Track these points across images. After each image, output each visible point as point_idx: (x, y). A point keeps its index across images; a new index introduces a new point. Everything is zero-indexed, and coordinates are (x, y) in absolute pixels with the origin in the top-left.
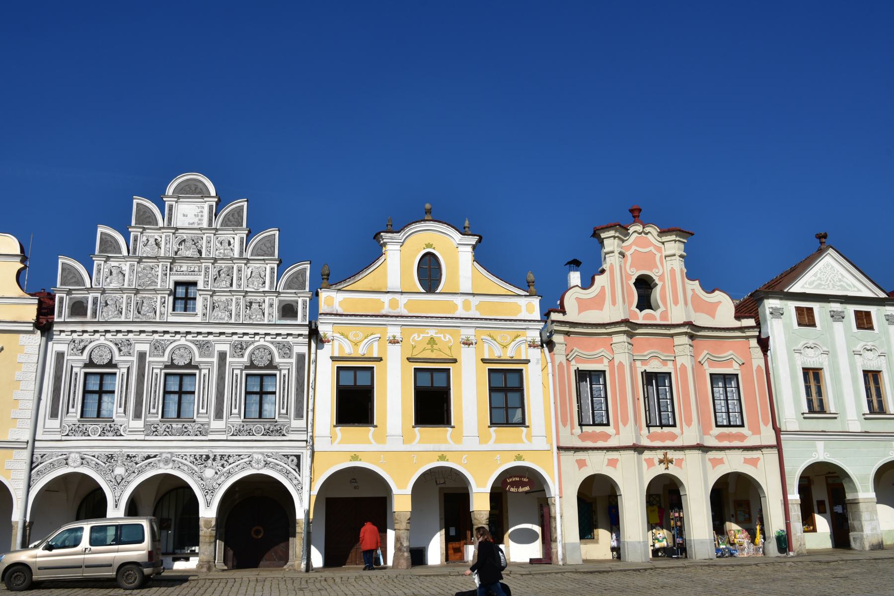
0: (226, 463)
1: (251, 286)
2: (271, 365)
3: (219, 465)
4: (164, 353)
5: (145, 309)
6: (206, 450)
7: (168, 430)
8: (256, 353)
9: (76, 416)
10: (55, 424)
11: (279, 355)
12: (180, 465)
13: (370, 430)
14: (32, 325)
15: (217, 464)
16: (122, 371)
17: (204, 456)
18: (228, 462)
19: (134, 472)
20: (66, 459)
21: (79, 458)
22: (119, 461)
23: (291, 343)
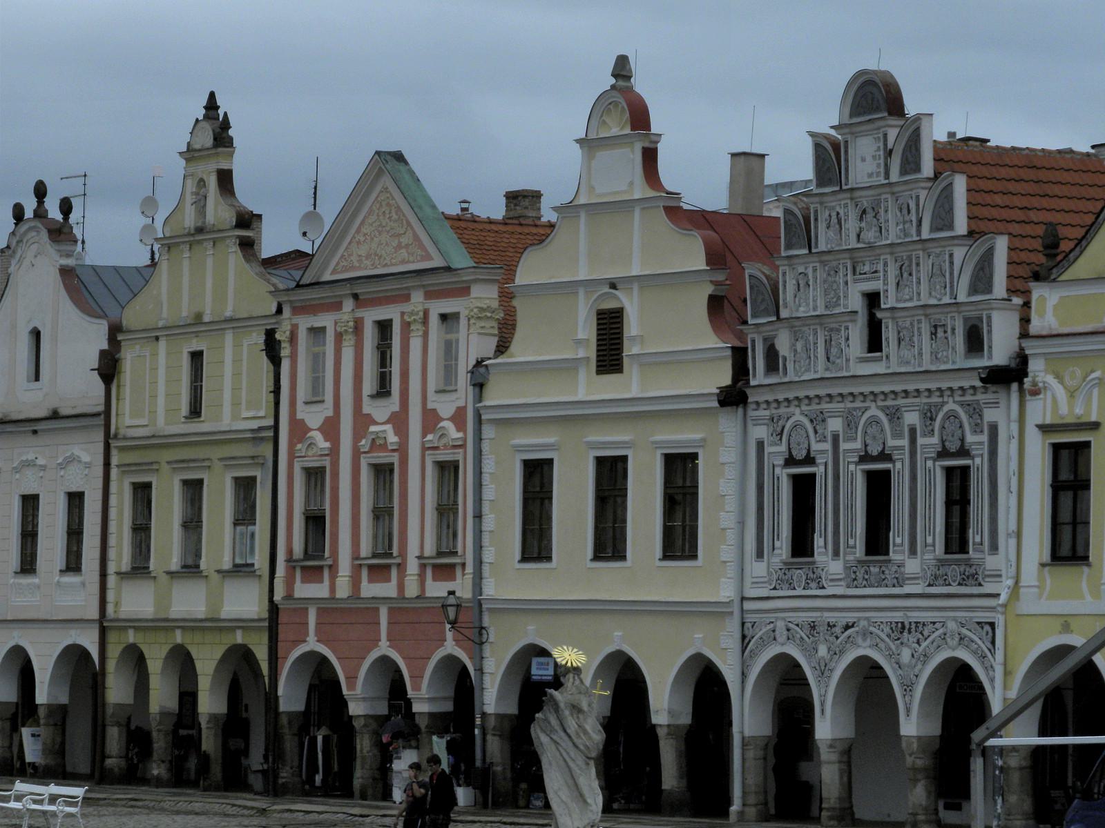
0: (921, 636)
1: (933, 293)
2: (963, 452)
3: (915, 640)
4: (856, 433)
5: (834, 351)
6: (900, 614)
7: (866, 577)
8: (946, 426)
9: (781, 554)
10: (758, 569)
11: (971, 427)
12: (878, 640)
13: (1082, 573)
14: (716, 398)
15: (912, 639)
16: (819, 470)
17: (900, 625)
18: (923, 635)
19: (835, 654)
20: (774, 631)
21: (784, 628)
22: (821, 634)
23: (981, 402)
